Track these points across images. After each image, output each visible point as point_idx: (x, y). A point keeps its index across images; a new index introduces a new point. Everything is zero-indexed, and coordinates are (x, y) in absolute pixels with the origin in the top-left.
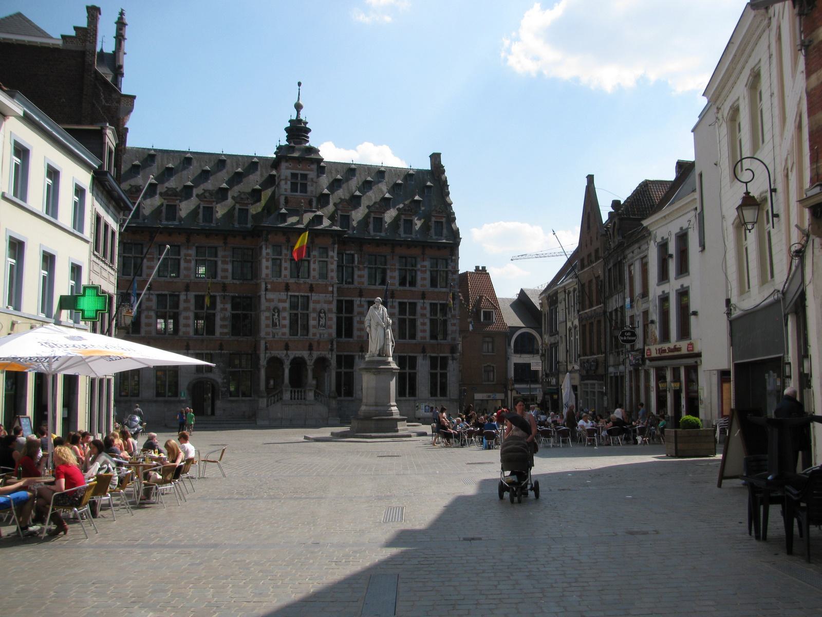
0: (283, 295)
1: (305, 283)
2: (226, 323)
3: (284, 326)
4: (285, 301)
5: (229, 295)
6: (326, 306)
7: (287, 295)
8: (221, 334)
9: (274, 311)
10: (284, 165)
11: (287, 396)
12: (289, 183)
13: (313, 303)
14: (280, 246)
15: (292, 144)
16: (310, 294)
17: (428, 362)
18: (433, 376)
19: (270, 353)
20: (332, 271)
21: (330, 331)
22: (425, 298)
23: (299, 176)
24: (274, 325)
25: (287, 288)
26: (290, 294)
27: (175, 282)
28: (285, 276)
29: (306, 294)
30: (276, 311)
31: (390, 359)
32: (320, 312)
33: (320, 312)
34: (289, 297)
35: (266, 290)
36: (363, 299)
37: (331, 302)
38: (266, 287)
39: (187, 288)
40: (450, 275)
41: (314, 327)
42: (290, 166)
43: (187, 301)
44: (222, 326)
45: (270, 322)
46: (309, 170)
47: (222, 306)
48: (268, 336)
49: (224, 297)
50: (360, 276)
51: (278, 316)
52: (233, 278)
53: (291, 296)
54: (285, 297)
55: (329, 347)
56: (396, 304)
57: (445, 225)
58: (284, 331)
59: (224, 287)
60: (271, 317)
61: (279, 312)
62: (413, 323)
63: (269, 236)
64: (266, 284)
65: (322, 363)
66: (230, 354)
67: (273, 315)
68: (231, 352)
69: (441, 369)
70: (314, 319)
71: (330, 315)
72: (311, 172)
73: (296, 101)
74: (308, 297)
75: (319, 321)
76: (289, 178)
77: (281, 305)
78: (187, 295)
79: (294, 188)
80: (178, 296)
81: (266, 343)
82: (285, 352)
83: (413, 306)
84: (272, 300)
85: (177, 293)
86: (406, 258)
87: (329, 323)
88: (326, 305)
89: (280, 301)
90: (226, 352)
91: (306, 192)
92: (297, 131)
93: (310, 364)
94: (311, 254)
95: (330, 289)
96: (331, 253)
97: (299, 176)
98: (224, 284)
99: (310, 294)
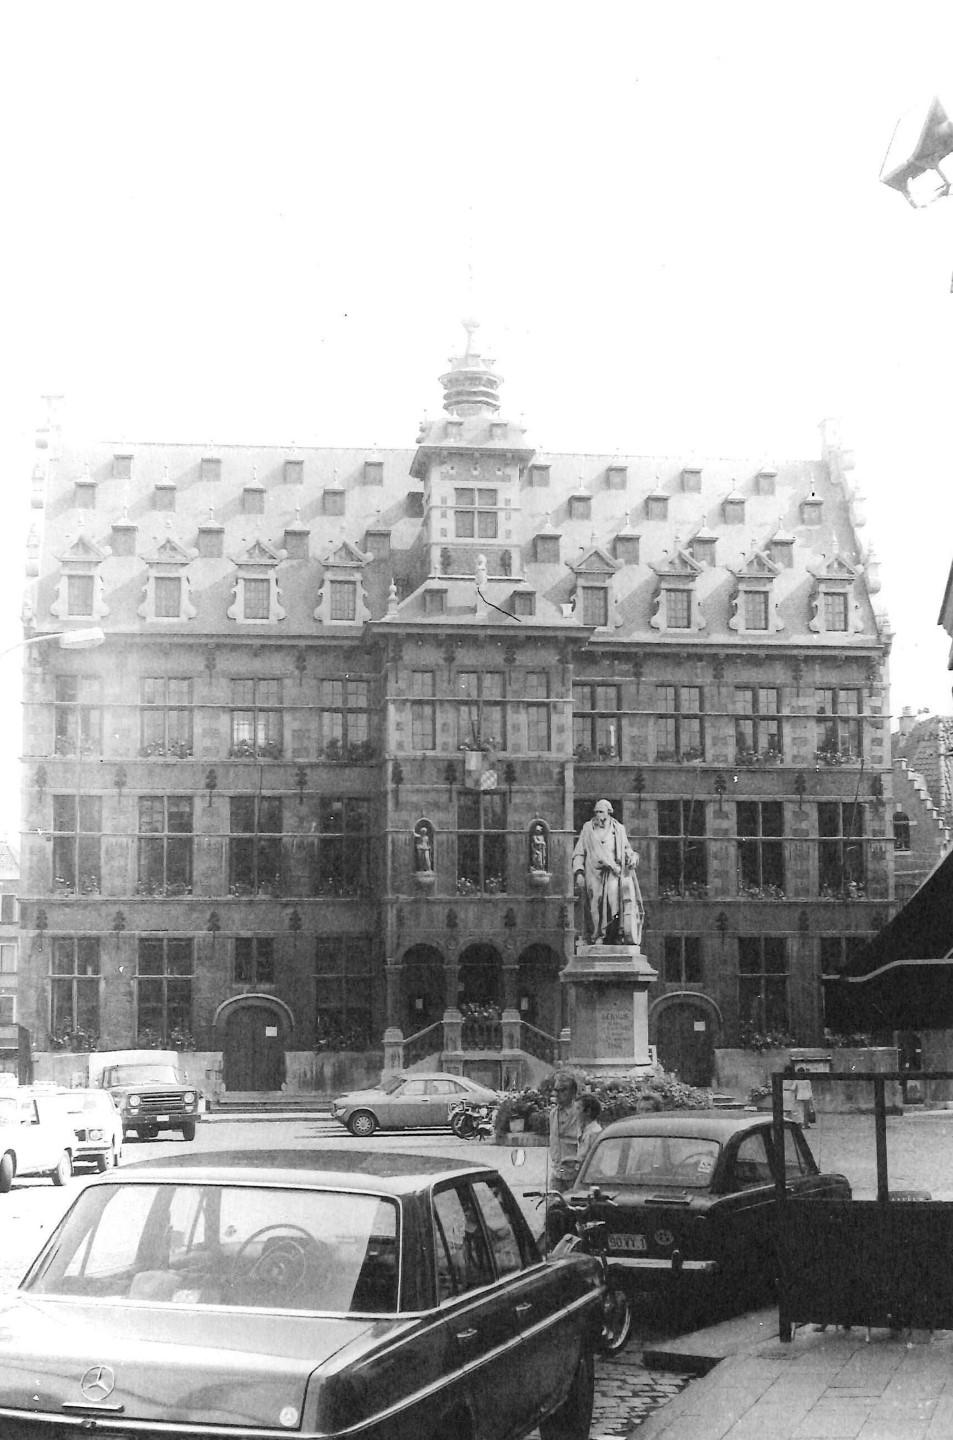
10: (435, 474)
12: (451, 514)
15: (455, 418)
22: (514, 779)
31: (634, 951)
32: (533, 832)
40: (867, 728)
42: (451, 472)
51: (430, 842)
56: (730, 808)
57: (852, 602)
62: (775, 850)
67: (417, 841)
75: (531, 853)
76: (452, 502)
83: (774, 809)
86: (777, 689)
92: (467, 389)
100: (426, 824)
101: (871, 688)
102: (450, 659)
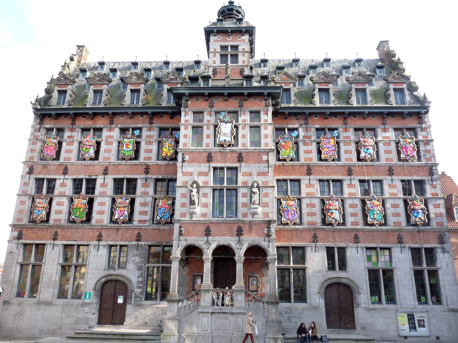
0: (204, 167)
1: (232, 152)
2: (146, 209)
3: (205, 205)
4: (206, 174)
5: (151, 178)
7: (209, 167)
8: (140, 221)
9: (192, 186)
11: (206, 299)
13: (243, 176)
14: (202, 113)
16: (238, 165)
17: (407, 255)
18: (418, 275)
19: (186, 240)
20: (266, 136)
21: (266, 210)
23: (229, 48)
24: (192, 203)
25: (209, 158)
26: (213, 165)
27: (94, 166)
28: (208, 145)
29: (234, 165)
30: (195, 185)
32: (252, 186)
33: (252, 186)
34: (212, 170)
35: (183, 161)
36: (312, 177)
38: (183, 158)
39: (106, 172)
41: (244, 205)
42: (219, 39)
43: (104, 185)
44: (141, 213)
45: (187, 200)
46: (240, 41)
47: (143, 189)
48: (184, 219)
49: (146, 180)
50: (306, 152)
51: (198, 192)
52: (158, 159)
53: (215, 169)
54: (206, 170)
55: (266, 231)
57: (407, 92)
58: (202, 210)
59: (147, 170)
60: (188, 195)
61: (198, 187)
63: (189, 102)
64: (183, 155)
65: (256, 254)
66: (150, 246)
68: (150, 243)
69: (428, 264)
70: (244, 195)
71: (265, 191)
74: (236, 169)
75: (251, 197)
76: (219, 49)
77: (201, 180)
78: (104, 178)
79: (224, 57)
80: (95, 180)
81: (180, 227)
82: (205, 238)
84: (191, 174)
85: (93, 177)
87: (264, 200)
88: (260, 177)
89: (200, 174)
90: (143, 243)
91: (238, 63)
93: (240, 254)
94: (240, 118)
95: (265, 158)
96: (263, 117)
97: (229, 48)
98: (147, 166)
99: (238, 165)
100: (195, 182)
101: (421, 128)
102: (211, 106)
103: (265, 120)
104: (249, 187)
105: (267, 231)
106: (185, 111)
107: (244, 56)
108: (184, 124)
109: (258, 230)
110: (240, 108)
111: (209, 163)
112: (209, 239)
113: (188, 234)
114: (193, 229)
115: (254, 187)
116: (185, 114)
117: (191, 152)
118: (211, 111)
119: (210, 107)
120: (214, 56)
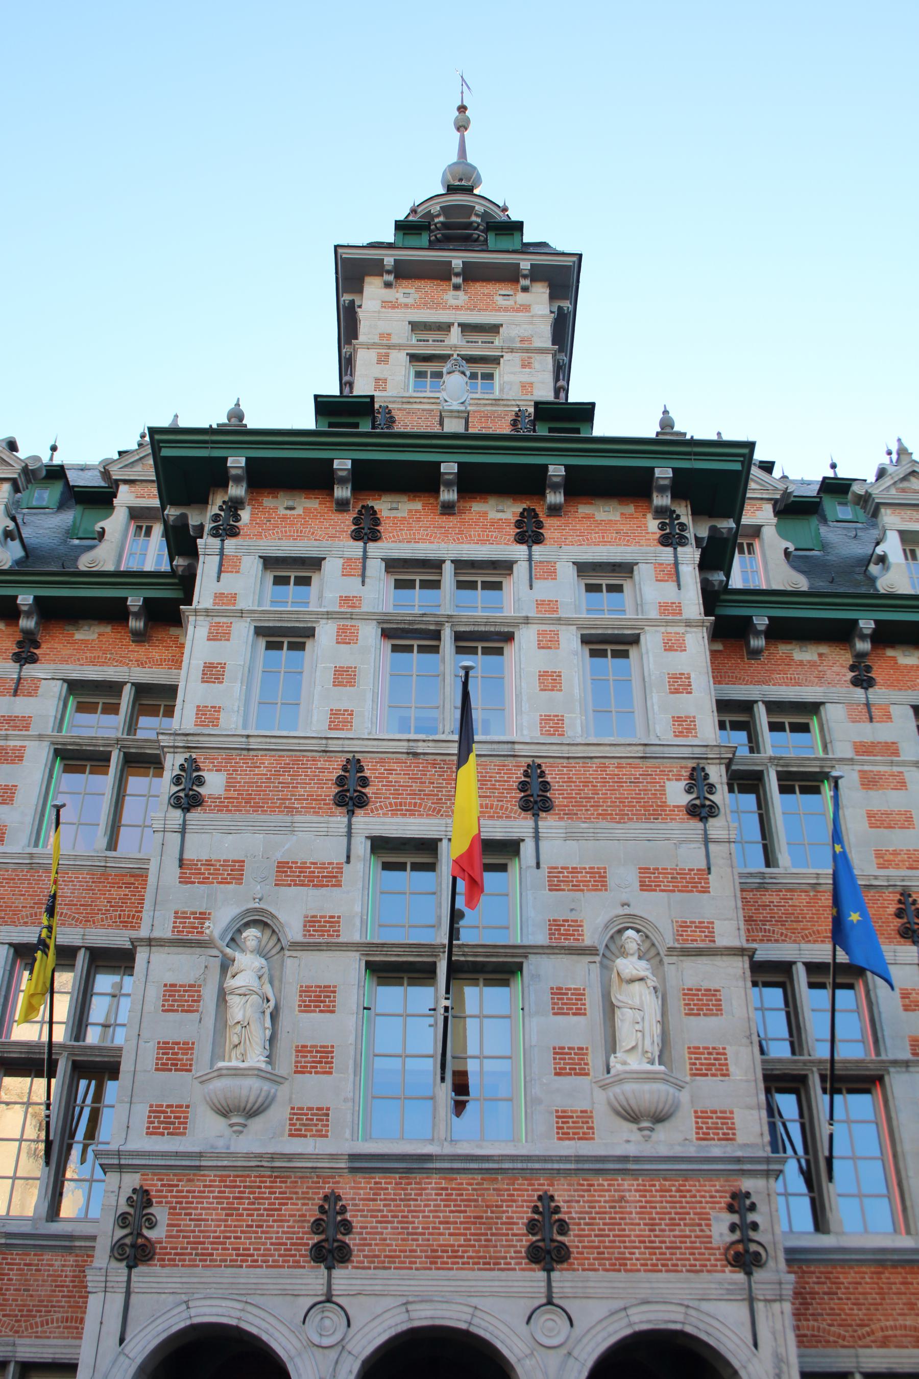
6: (661, 911)
13: (554, 887)
26: (370, 823)
33: (612, 947)
37: (696, 882)
54: (329, 850)
55: (720, 1229)
72: (521, 316)
73: (454, 158)
76: (401, 332)
82: (313, 1279)
84: (233, 871)
89: (291, 873)
100: (260, 920)
102: (367, 530)
103: (664, 608)
104: (590, 951)
105: (733, 1228)
106: (221, 554)
107: (526, 364)
108: (207, 612)
109: (673, 1224)
110: (524, 548)
111: (351, 813)
112: (337, 1288)
113: (198, 1253)
114: (230, 1211)
115: (624, 953)
116: (221, 565)
117: (242, 751)
118: (365, 557)
119: (357, 536)
120: (379, 362)
